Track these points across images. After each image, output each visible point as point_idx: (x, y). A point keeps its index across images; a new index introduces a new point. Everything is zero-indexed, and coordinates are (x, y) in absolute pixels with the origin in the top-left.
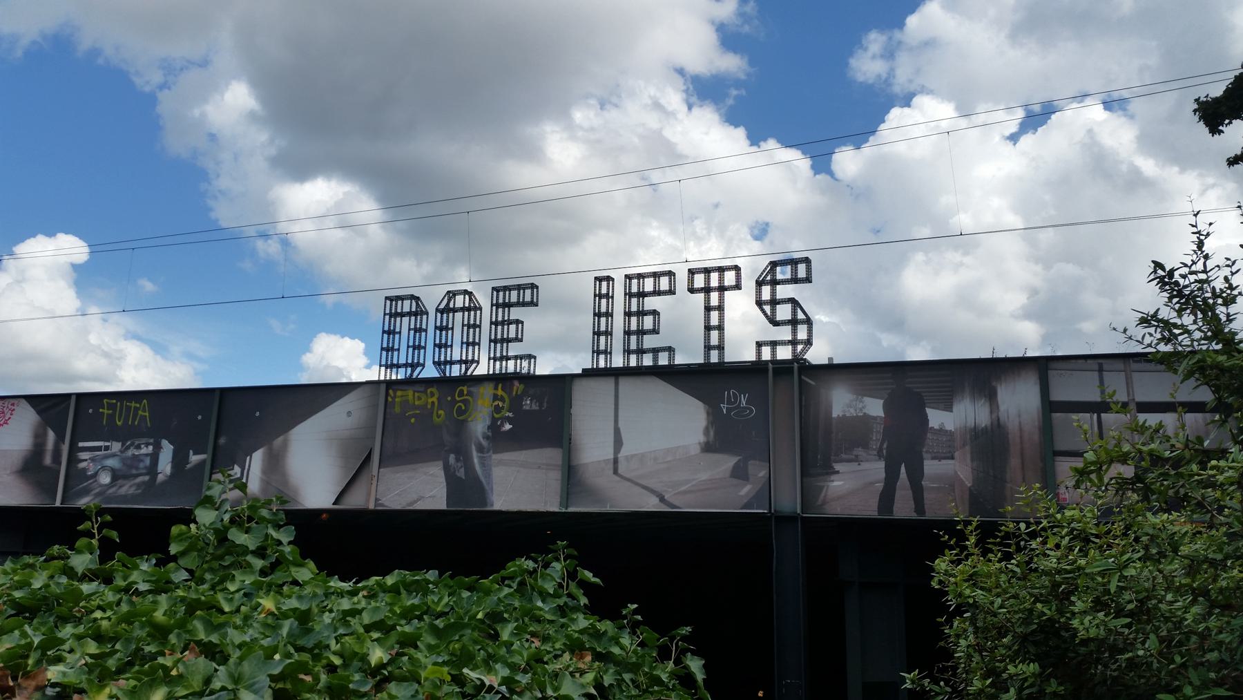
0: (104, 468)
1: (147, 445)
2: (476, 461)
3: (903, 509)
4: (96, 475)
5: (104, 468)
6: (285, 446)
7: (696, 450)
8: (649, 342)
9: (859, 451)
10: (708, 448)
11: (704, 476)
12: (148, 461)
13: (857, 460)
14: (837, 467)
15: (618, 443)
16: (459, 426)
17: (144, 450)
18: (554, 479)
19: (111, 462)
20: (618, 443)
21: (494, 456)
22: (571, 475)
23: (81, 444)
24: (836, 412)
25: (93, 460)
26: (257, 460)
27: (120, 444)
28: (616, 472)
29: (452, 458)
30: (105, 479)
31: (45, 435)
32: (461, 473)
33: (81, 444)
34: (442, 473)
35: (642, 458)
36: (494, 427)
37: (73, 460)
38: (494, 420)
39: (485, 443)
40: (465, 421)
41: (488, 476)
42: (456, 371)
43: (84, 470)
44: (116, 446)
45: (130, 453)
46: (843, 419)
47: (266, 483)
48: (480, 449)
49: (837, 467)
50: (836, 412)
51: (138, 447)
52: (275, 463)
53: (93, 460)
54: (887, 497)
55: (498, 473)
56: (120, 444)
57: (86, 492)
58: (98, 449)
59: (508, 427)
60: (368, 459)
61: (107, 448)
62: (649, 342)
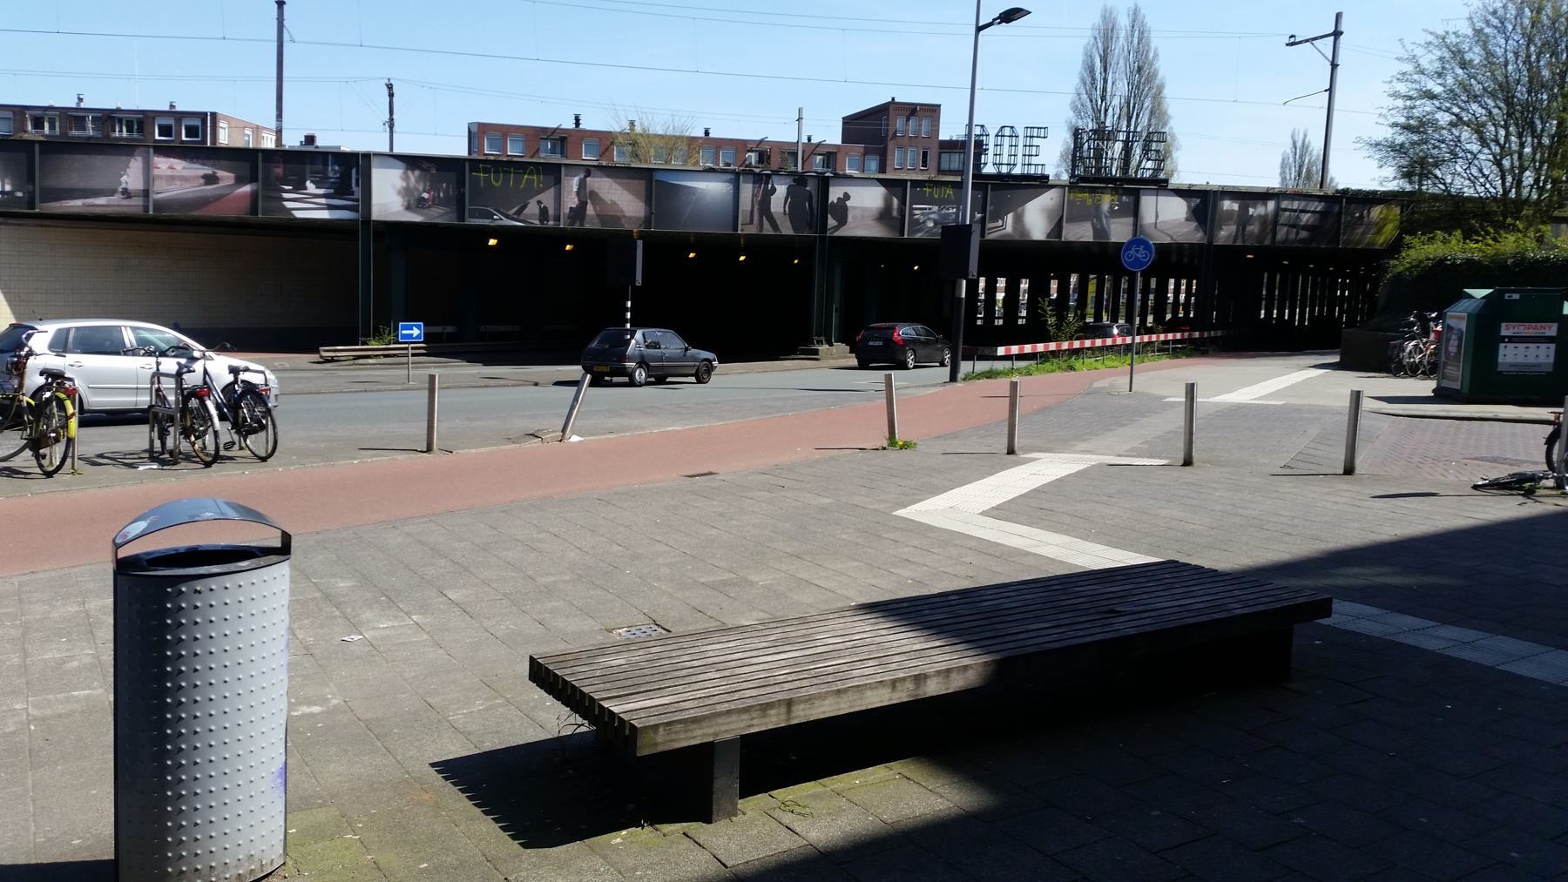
0: (929, 219)
1: (953, 208)
2: (1104, 222)
3: (1239, 243)
4: (925, 222)
5: (929, 219)
6: (1023, 211)
7: (1183, 220)
8: (1034, 160)
9: (1230, 222)
10: (1187, 219)
11: (1186, 230)
12: (954, 216)
13: (1229, 225)
14: (1223, 227)
15: (1157, 217)
16: (1098, 207)
17: (951, 211)
18: (1130, 229)
19: (932, 216)
20: (1157, 217)
21: (1113, 220)
22: (1136, 225)
23: (914, 206)
24: (1225, 208)
25: (922, 214)
26: (1010, 218)
27: (937, 208)
28: (1156, 227)
29: (1095, 220)
30: (931, 224)
31: (892, 201)
32: (1099, 227)
33: (914, 206)
34: (1091, 226)
35: (1165, 223)
36: (1111, 208)
37: (912, 215)
38: (1111, 205)
39: (1108, 214)
40: (1100, 205)
41: (1108, 225)
42: (1004, 170)
43: (918, 219)
44: (935, 208)
45: (944, 211)
46: (1226, 210)
47: (1015, 228)
48: (1106, 217)
49: (1223, 227)
50: (1225, 208)
51: (948, 209)
52: (1019, 220)
53: (922, 214)
54: (1235, 239)
55: (1112, 226)
56: (937, 208)
57: (919, 231)
58: (925, 209)
59: (1117, 208)
60: (1061, 219)
61: (930, 209)
62: (1034, 160)
